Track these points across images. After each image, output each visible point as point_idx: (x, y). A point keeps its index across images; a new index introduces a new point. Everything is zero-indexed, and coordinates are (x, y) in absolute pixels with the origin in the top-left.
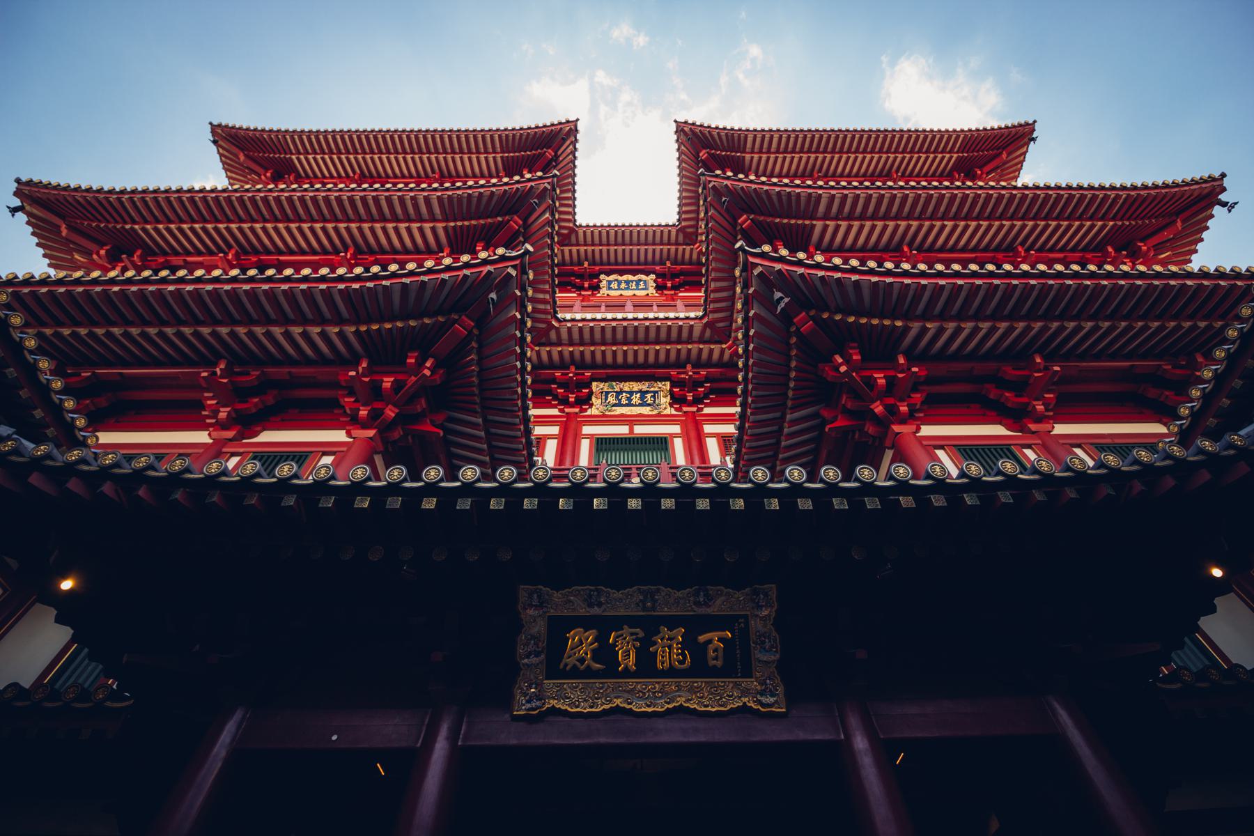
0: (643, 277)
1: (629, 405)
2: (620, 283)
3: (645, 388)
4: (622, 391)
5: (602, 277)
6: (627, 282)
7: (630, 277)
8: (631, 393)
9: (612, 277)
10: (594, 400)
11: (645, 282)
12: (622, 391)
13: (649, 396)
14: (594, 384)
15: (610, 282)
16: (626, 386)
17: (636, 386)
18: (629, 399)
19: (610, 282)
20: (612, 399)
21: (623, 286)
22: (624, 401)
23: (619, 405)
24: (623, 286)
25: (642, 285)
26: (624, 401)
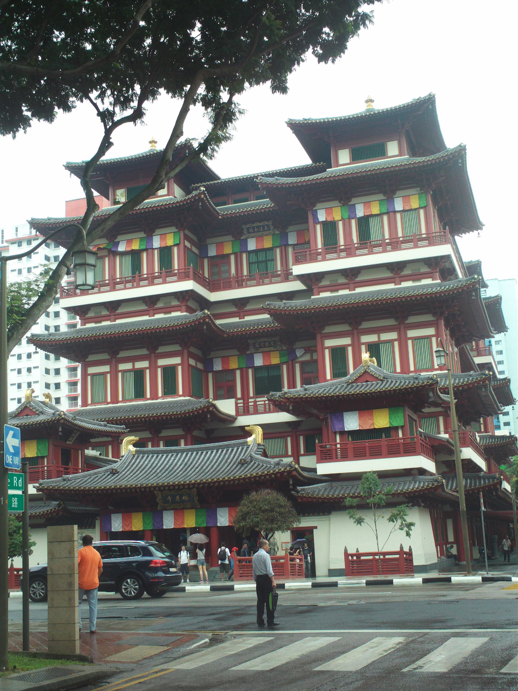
0: (266, 223)
1: (265, 347)
2: (253, 228)
3: (270, 341)
4: (260, 342)
5: (245, 227)
6: (258, 227)
7: (259, 224)
8: (264, 342)
9: (248, 226)
10: (250, 347)
11: (268, 226)
12: (260, 342)
13: (272, 343)
14: (249, 340)
15: (248, 229)
16: (262, 340)
17: (266, 340)
18: (264, 345)
19: (248, 229)
20: (257, 346)
21: (256, 230)
22: (262, 346)
23: (261, 347)
24: (256, 230)
25: (266, 229)
26: (262, 346)
